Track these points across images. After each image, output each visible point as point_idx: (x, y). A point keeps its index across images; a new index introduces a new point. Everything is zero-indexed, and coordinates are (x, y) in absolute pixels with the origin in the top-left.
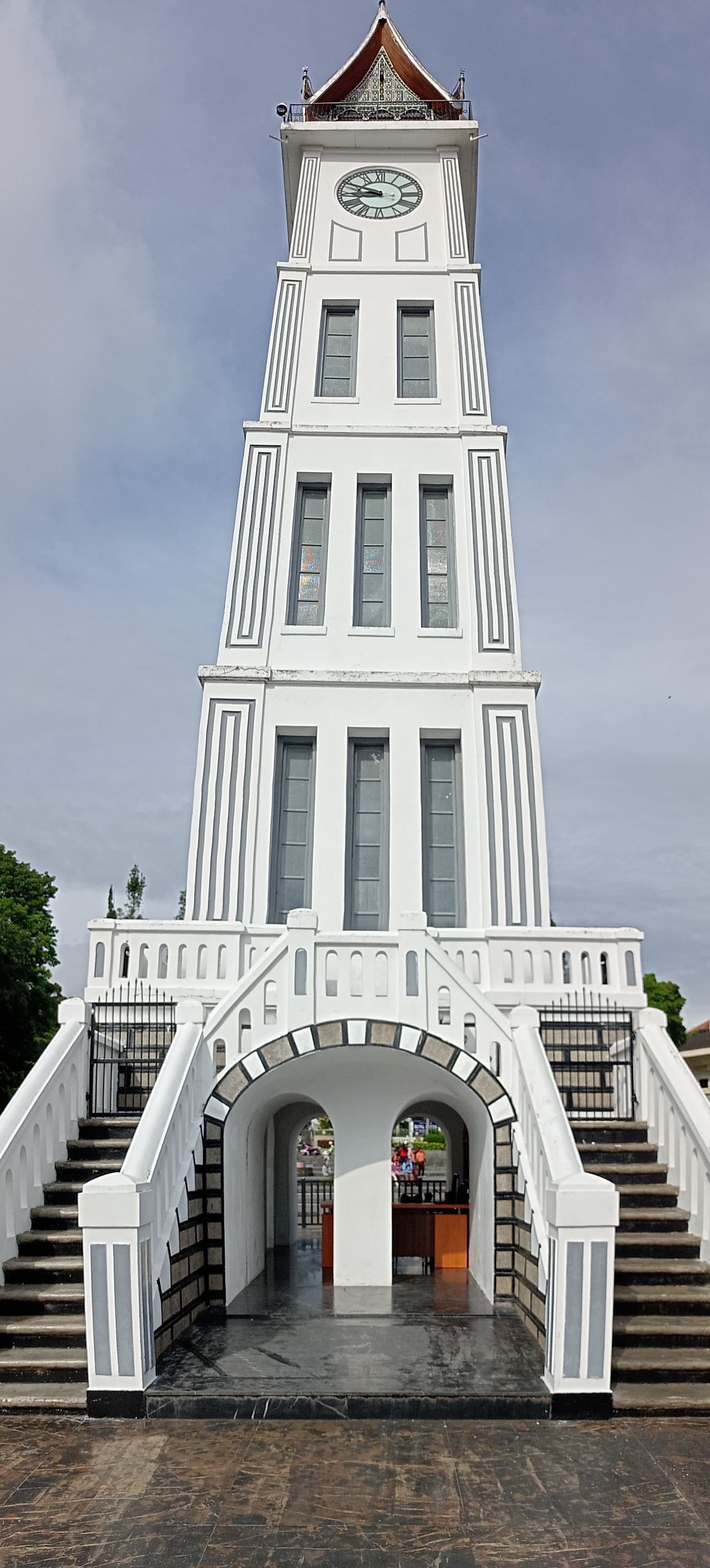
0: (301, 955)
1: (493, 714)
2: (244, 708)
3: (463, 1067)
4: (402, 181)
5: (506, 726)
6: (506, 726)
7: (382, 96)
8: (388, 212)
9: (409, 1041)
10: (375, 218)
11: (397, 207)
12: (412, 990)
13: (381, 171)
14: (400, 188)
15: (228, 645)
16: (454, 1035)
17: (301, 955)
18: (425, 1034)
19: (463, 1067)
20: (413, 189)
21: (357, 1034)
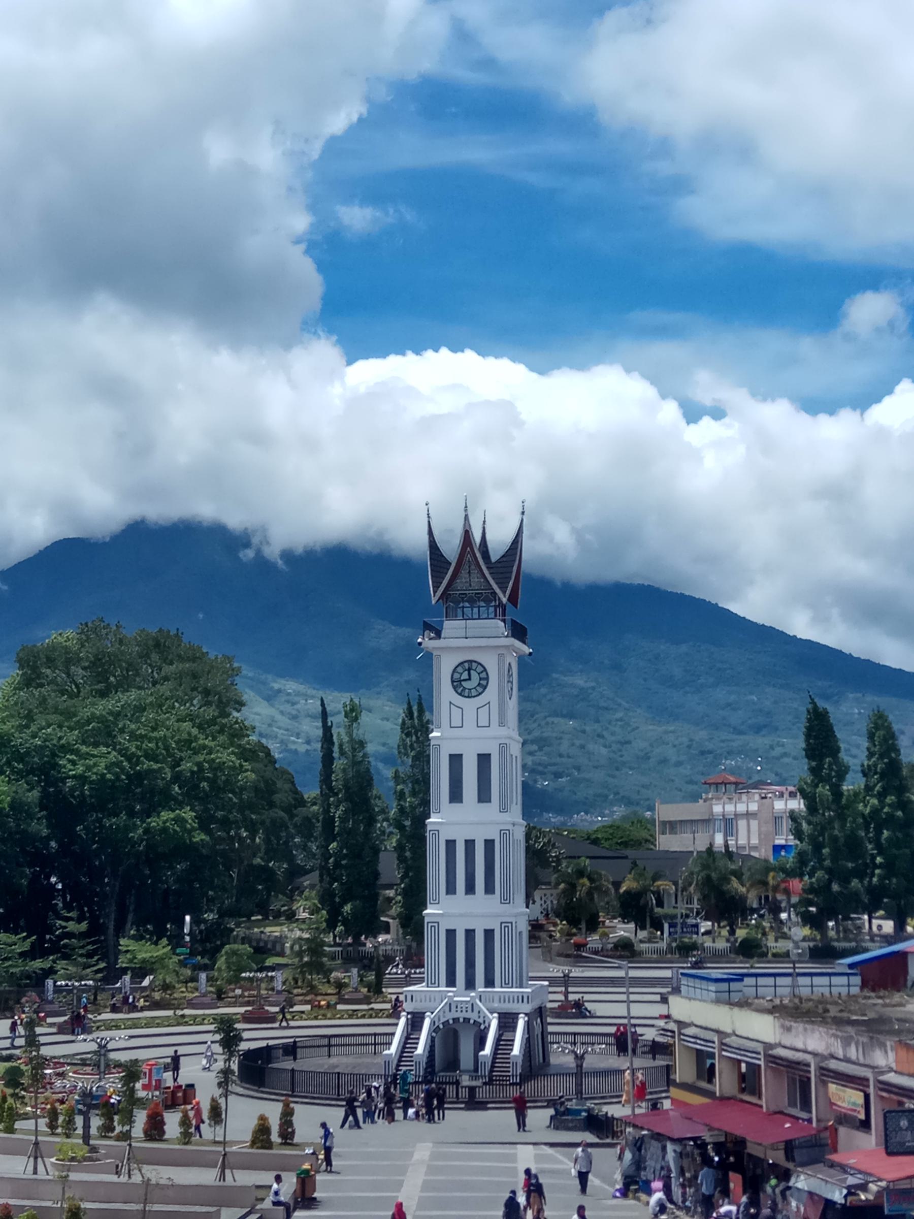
0: (450, 1004)
1: (503, 925)
2: (436, 925)
3: (482, 1027)
4: (480, 669)
5: (506, 929)
6: (506, 929)
7: (470, 585)
8: (474, 693)
9: (472, 1021)
10: (468, 697)
11: (478, 688)
12: (472, 1010)
13: (471, 662)
14: (479, 674)
15: (430, 903)
16: (481, 1020)
17: (450, 1004)
18: (475, 1021)
19: (482, 1027)
20: (483, 675)
21: (461, 1020)
